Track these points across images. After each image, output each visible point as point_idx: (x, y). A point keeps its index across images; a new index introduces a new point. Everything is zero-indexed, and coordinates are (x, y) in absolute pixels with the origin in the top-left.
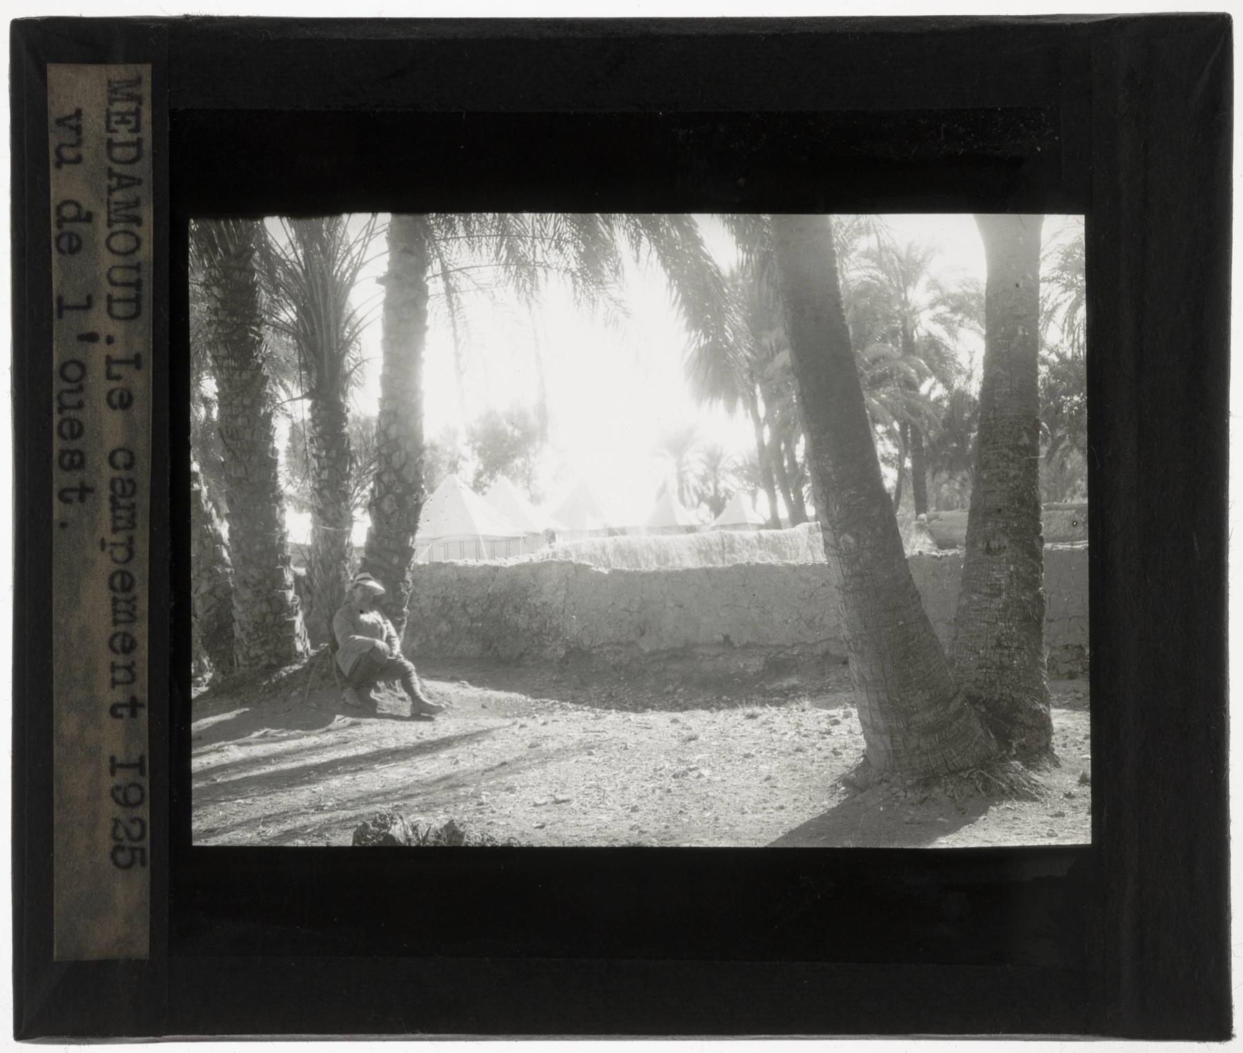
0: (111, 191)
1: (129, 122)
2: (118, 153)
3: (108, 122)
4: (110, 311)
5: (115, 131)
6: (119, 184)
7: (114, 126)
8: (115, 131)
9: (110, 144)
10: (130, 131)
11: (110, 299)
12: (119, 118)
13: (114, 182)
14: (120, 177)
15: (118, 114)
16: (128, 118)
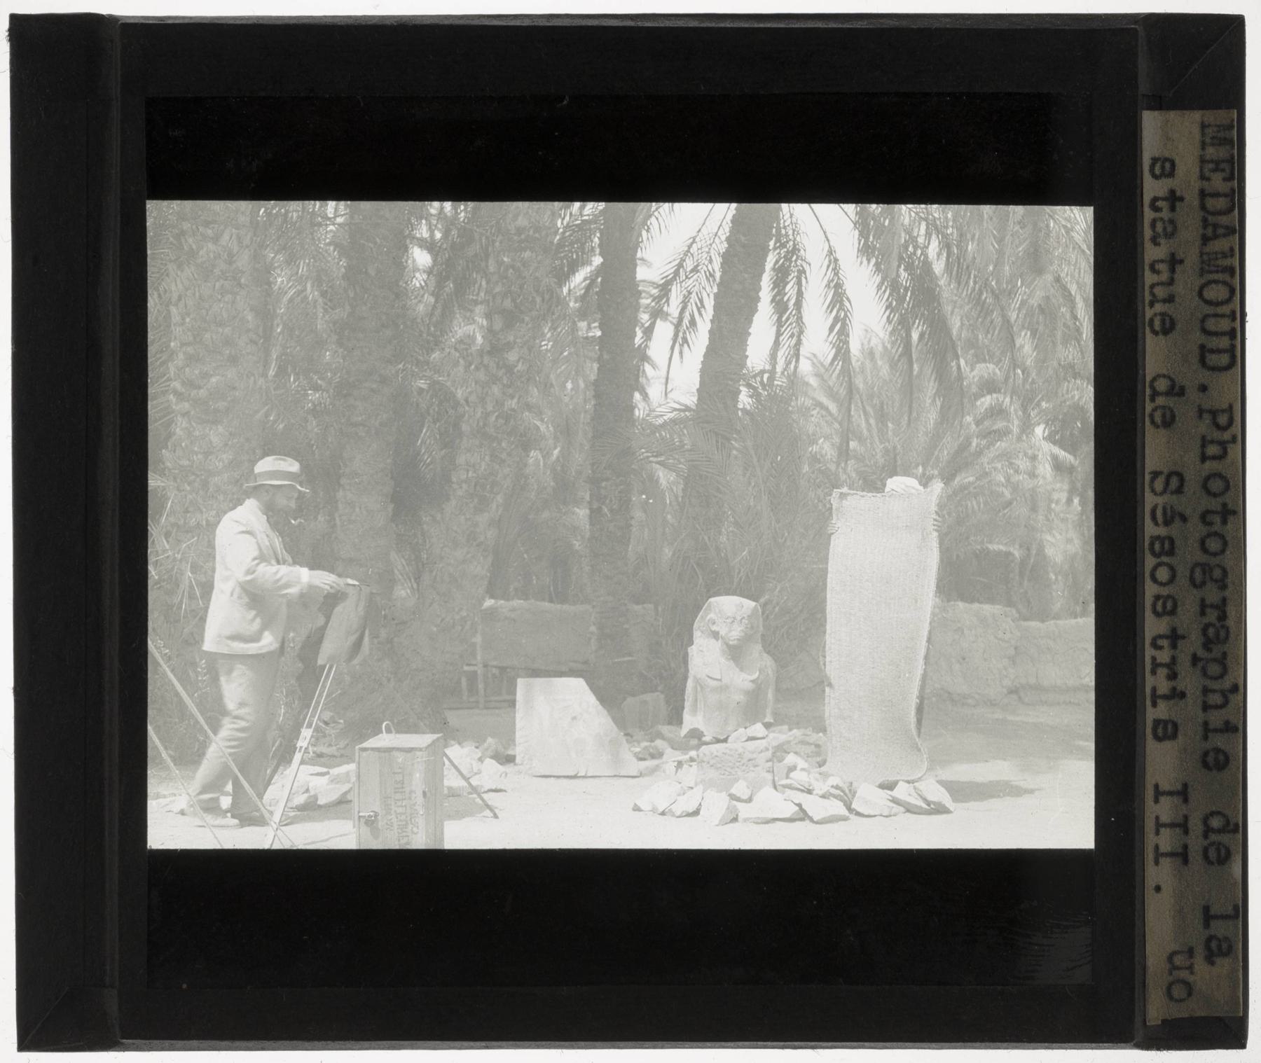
0: (1205, 240)
1: (1223, 170)
2: (1211, 203)
3: (1201, 170)
4: (1203, 361)
5: (1208, 179)
6: (1214, 231)
7: (1207, 174)
8: (1208, 179)
9: (1203, 194)
10: (1224, 180)
11: (1202, 347)
12: (1211, 166)
13: (1209, 231)
14: (1215, 226)
15: (1212, 161)
16: (1223, 166)
